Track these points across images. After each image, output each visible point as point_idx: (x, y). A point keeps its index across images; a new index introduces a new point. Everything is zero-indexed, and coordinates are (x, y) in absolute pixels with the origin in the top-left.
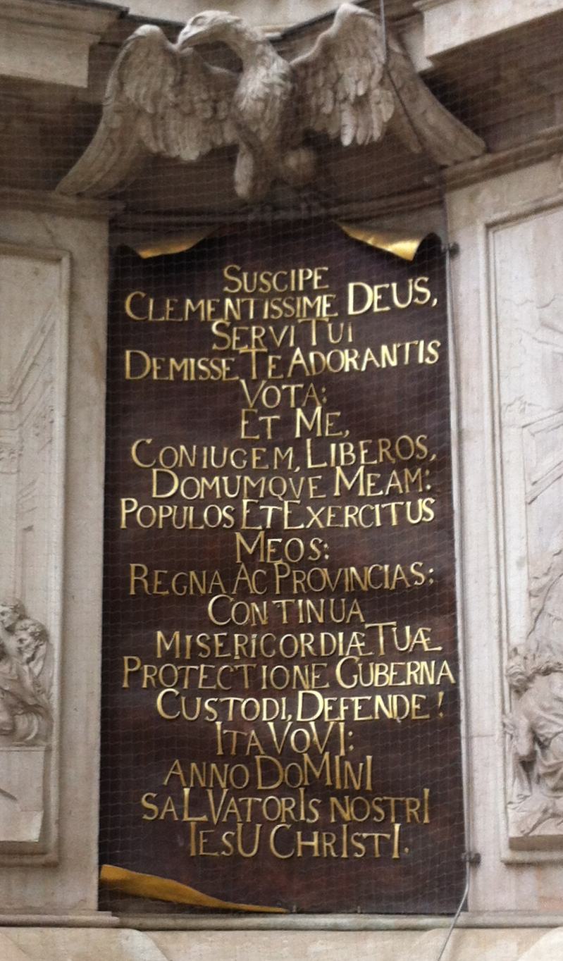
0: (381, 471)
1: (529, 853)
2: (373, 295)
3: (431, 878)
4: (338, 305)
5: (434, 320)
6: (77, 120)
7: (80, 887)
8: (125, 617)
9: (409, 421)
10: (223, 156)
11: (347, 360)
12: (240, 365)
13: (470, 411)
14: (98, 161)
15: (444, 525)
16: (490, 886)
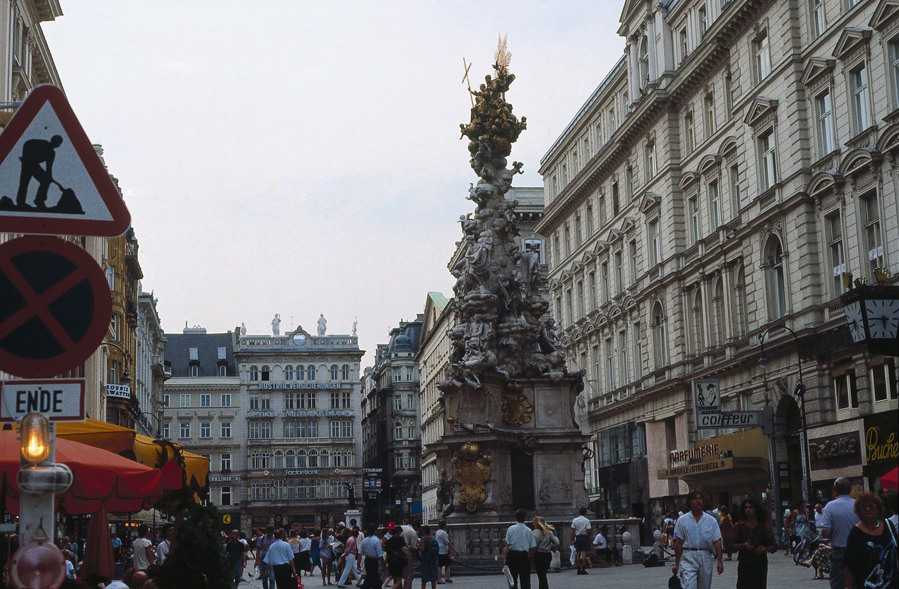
1: (541, 505)
16: (537, 508)
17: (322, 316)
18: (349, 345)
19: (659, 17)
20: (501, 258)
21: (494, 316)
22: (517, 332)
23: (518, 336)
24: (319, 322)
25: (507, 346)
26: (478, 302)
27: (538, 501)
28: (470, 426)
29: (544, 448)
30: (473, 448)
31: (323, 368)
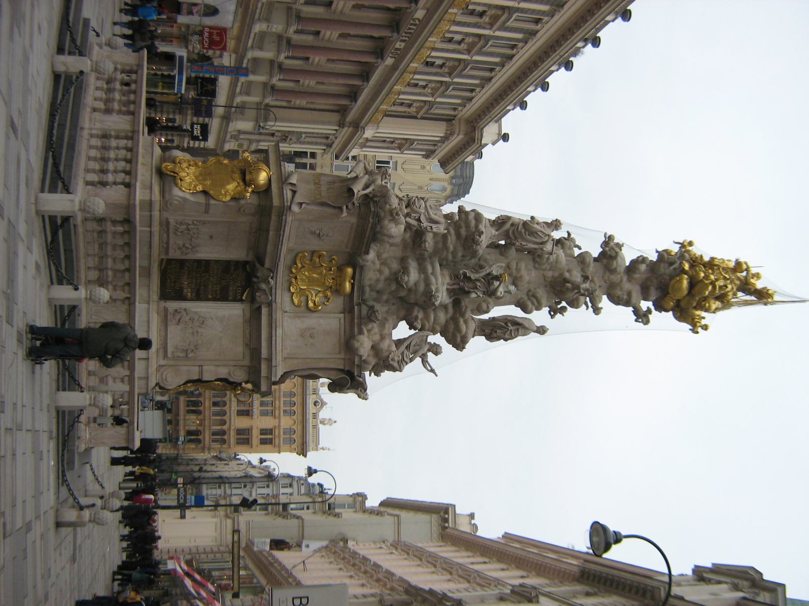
0: (216, 291)
1: (166, 310)
2: (240, 291)
3: (165, 295)
4: (238, 287)
5: (235, 300)
6: (262, 265)
7: (163, 257)
8: (199, 262)
9: (222, 297)
10: (258, 278)
11: (231, 288)
12: (232, 274)
13: (220, 304)
14: (258, 265)
15: (208, 300)
16: (163, 304)
17: (335, 422)
18: (311, 444)
19: (741, 594)
20: (526, 278)
21: (451, 248)
22: (428, 284)
23: (422, 288)
24: (330, 420)
25: (405, 270)
26: (473, 223)
27: (173, 305)
28: (294, 180)
29: (255, 315)
30: (263, 177)
31: (292, 422)
